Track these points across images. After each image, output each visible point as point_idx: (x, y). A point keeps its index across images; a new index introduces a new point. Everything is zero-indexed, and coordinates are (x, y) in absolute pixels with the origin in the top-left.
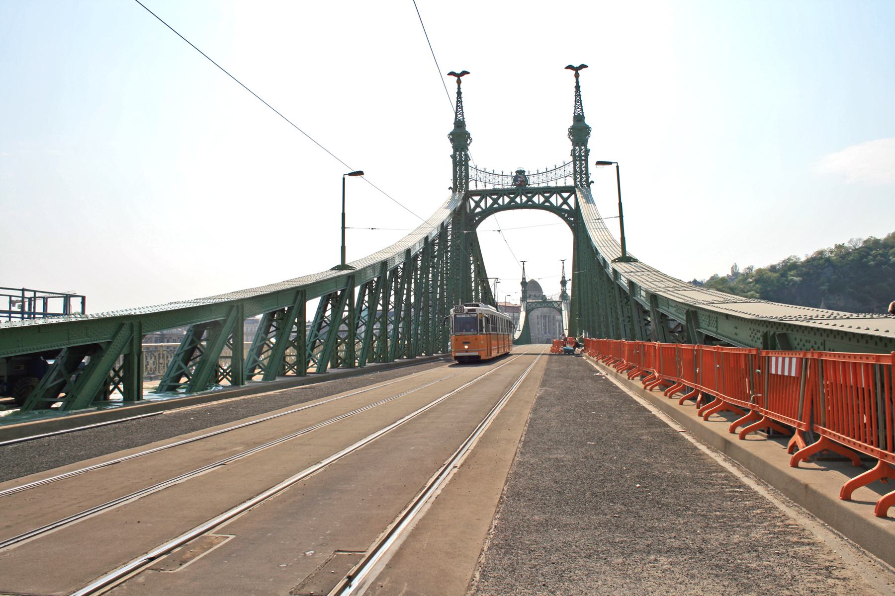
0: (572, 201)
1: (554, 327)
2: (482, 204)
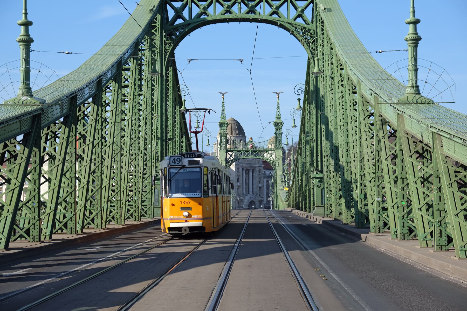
0: (308, 14)
1: (260, 185)
2: (186, 13)
